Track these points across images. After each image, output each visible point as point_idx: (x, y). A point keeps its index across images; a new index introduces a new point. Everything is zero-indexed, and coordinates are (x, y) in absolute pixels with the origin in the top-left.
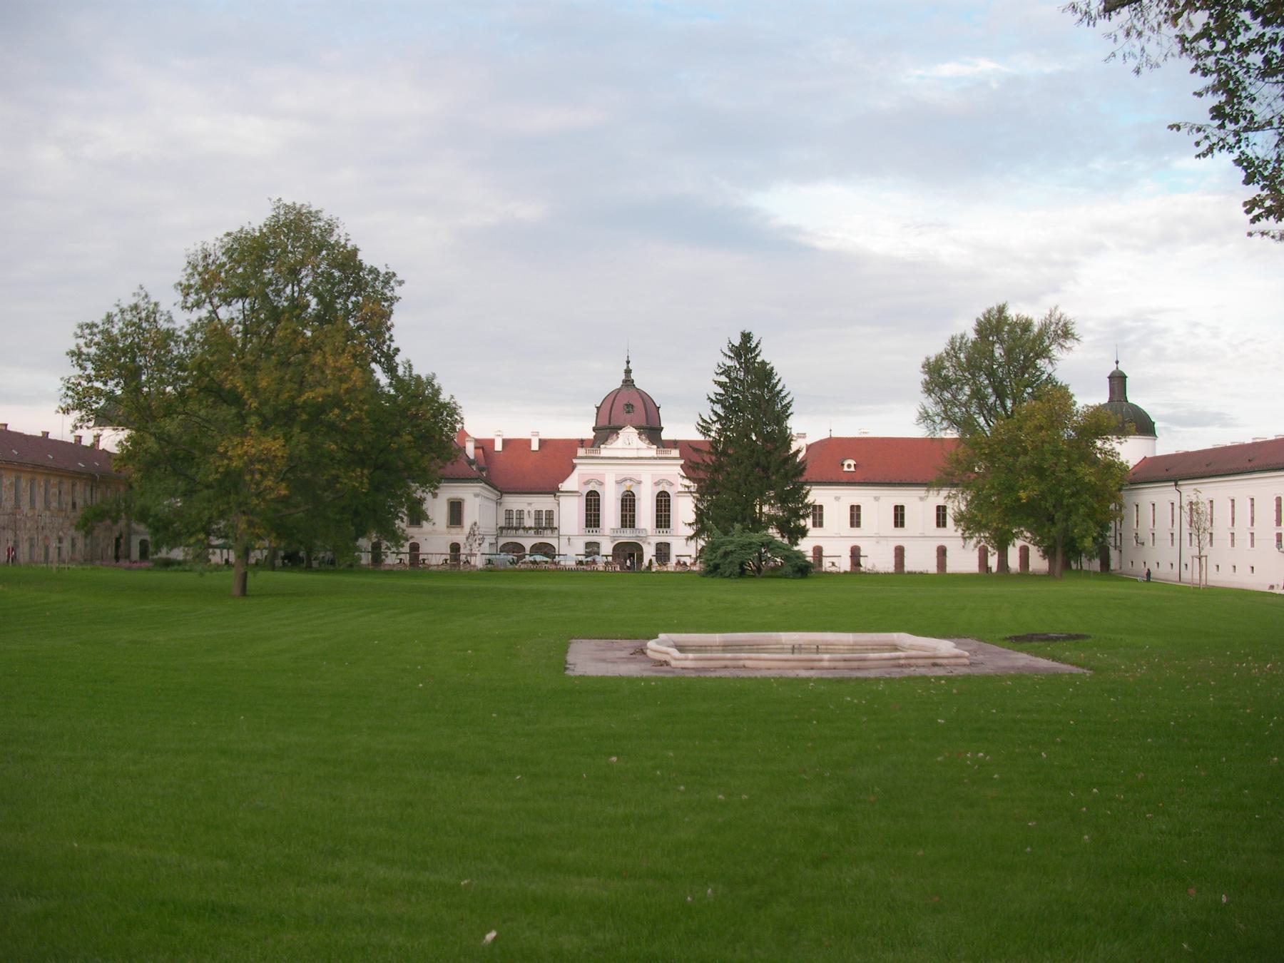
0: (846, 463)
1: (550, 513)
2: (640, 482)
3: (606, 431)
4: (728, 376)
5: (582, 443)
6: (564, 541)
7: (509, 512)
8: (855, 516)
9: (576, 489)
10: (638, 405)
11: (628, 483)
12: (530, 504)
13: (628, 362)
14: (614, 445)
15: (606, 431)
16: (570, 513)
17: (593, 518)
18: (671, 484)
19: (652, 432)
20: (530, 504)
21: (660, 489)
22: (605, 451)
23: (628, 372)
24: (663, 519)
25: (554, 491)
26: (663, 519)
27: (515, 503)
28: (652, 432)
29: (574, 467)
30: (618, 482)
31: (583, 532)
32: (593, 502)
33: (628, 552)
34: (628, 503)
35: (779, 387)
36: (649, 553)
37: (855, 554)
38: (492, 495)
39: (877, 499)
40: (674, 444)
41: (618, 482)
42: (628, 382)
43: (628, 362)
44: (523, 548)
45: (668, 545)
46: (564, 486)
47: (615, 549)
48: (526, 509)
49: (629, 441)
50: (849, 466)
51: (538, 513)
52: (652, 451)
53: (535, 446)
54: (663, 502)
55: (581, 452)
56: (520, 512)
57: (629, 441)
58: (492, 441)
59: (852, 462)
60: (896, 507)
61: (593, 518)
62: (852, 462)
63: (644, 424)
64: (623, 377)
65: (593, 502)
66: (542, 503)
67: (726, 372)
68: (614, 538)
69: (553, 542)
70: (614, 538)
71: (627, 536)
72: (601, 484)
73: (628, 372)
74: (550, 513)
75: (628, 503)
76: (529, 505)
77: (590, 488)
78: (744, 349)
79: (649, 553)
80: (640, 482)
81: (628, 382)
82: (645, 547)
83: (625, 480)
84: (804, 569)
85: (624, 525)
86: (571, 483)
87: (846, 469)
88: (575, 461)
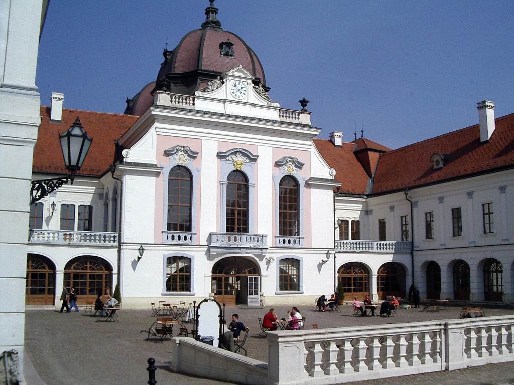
6: (129, 254)
9: (152, 160)
11: (239, 159)
14: (220, 93)
29: (152, 120)
31: (162, 238)
34: (238, 190)
41: (221, 156)
44: (52, 266)
45: (296, 263)
46: (132, 155)
47: (217, 268)
69: (109, 255)
72: (193, 155)
80: (253, 159)
82: (262, 264)
83: (235, 152)
85: (230, 229)
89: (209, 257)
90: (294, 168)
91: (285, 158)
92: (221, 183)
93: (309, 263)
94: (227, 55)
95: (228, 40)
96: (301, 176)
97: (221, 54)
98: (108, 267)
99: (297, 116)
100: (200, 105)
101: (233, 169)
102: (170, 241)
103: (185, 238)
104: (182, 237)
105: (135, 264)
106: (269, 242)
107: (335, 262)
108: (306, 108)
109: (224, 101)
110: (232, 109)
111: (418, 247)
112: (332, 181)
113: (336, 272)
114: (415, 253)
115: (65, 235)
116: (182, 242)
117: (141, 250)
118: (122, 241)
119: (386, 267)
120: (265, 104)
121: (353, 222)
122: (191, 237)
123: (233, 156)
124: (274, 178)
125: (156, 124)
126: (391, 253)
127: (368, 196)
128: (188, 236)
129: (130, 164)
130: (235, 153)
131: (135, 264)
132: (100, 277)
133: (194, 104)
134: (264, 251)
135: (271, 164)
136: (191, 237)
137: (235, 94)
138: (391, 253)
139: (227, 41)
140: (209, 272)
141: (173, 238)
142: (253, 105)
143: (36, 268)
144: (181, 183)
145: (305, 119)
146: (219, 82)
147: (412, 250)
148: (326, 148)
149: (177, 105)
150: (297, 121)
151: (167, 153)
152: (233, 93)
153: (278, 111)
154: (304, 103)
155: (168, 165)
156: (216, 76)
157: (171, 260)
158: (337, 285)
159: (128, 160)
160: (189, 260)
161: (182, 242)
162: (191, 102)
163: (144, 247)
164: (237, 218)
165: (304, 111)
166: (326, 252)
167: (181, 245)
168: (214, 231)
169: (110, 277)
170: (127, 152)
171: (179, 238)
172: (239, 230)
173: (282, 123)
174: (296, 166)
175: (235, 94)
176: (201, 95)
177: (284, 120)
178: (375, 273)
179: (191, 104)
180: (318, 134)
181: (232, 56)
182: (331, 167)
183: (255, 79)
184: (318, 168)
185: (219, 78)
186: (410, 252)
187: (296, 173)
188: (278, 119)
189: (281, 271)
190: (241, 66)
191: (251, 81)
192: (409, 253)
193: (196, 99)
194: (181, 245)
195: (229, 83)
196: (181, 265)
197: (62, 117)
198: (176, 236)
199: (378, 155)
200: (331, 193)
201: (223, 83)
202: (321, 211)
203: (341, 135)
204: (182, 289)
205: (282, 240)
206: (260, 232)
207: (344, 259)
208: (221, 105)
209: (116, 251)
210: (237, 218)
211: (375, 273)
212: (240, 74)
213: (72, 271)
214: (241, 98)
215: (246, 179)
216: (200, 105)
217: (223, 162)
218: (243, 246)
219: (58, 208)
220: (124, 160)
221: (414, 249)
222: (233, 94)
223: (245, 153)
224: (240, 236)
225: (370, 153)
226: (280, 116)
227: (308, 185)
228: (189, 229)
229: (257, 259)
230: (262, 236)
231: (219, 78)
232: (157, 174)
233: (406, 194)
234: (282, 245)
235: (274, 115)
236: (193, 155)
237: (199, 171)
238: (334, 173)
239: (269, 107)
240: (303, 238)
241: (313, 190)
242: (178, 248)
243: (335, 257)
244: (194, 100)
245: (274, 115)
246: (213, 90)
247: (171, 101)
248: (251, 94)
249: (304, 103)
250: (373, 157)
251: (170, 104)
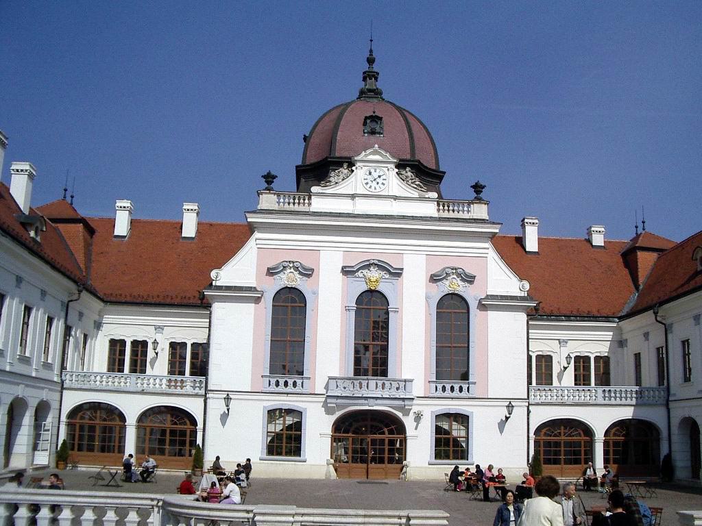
2: (397, 274)
6: (216, 406)
11: (374, 274)
13: (371, 61)
17: (287, 352)
18: (469, 279)
20: (159, 328)
21: (445, 287)
24: (453, 358)
26: (453, 358)
30: (346, 271)
31: (263, 385)
33: (369, 438)
41: (346, 271)
43: (371, 61)
44: (122, 417)
45: (463, 419)
46: (225, 276)
47: (339, 426)
51: (176, 348)
61: (287, 352)
69: (193, 406)
72: (307, 273)
73: (370, 75)
80: (397, 274)
82: (408, 422)
86: (241, 269)
89: (329, 411)
90: (461, 283)
91: (444, 269)
92: (347, 309)
93: (483, 420)
94: (373, 132)
95: (374, 112)
96: (472, 294)
97: (364, 133)
98: (194, 422)
99: (466, 209)
100: (318, 204)
101: (365, 288)
102: (273, 388)
103: (295, 384)
104: (290, 382)
105: (224, 417)
106: (418, 389)
107: (528, 419)
108: (481, 195)
109: (353, 196)
110: (363, 206)
111: (675, 395)
112: (522, 299)
113: (532, 435)
114: (671, 405)
115: (170, 381)
116: (290, 389)
117: (228, 399)
118: (209, 388)
119: (620, 425)
120: (416, 194)
121: (597, 358)
122: (302, 383)
123: (365, 271)
124: (427, 298)
125: (257, 235)
126: (632, 405)
127: (621, 318)
128: (299, 382)
129: (219, 288)
130: (368, 266)
131: (224, 417)
132: (183, 433)
133: (310, 204)
134: (407, 402)
135: (423, 278)
136: (302, 383)
137: (369, 186)
138: (632, 405)
139: (372, 114)
140: (328, 430)
141: (277, 384)
142: (396, 198)
143: (175, 424)
144: (290, 310)
145: (480, 211)
146: (346, 171)
147: (668, 401)
148: (511, 249)
149: (287, 207)
150: (466, 216)
151: (271, 272)
152: (367, 184)
153: (436, 203)
154: (478, 188)
155: (271, 287)
157: (272, 414)
158: (532, 453)
159: (218, 284)
160: (299, 413)
161: (290, 389)
162: (307, 201)
163: (231, 396)
164: (372, 353)
165: (479, 200)
166: (507, 404)
167: (288, 394)
168: (337, 375)
169: (194, 433)
170: (217, 273)
171: (286, 384)
172: (375, 374)
173: (441, 219)
174: (463, 280)
175: (369, 186)
176: (321, 191)
177: (446, 215)
178: (599, 436)
179: (306, 205)
180: (497, 231)
181: (380, 133)
182: (521, 279)
183: (400, 160)
184: (500, 279)
185: (345, 165)
186: (665, 402)
187: (460, 287)
188: (436, 215)
189: (439, 430)
190: (376, 146)
191: (393, 166)
192: (661, 405)
193: (313, 197)
194: (288, 394)
195: (360, 172)
196: (290, 420)
197: (198, 232)
198: (282, 382)
199: (655, 255)
200: (523, 317)
201: (353, 171)
202: (503, 343)
203: (603, 229)
204: (289, 453)
205: (440, 387)
207: (542, 415)
208: (349, 201)
209: (202, 400)
210: (372, 353)
211: (599, 436)
212: (377, 157)
214: (378, 189)
216: (318, 204)
217: (351, 279)
218: (374, 396)
220: (214, 284)
221: (671, 399)
222: (373, 184)
223: (381, 266)
224: (367, 381)
225: (639, 254)
226: (439, 210)
227: (482, 307)
228: (302, 373)
229: (399, 414)
230: (405, 381)
231: (345, 165)
232: (257, 300)
233: (656, 314)
234: (440, 393)
235: (430, 209)
236: (307, 273)
237: (315, 293)
238: (527, 286)
239: (421, 199)
240: (475, 383)
241: (492, 314)
242: (284, 398)
243: (529, 412)
244: (310, 198)
245: (430, 209)
246: (337, 183)
247: (279, 203)
248: (393, 182)
249: (478, 188)
250: (646, 261)
251: (276, 207)
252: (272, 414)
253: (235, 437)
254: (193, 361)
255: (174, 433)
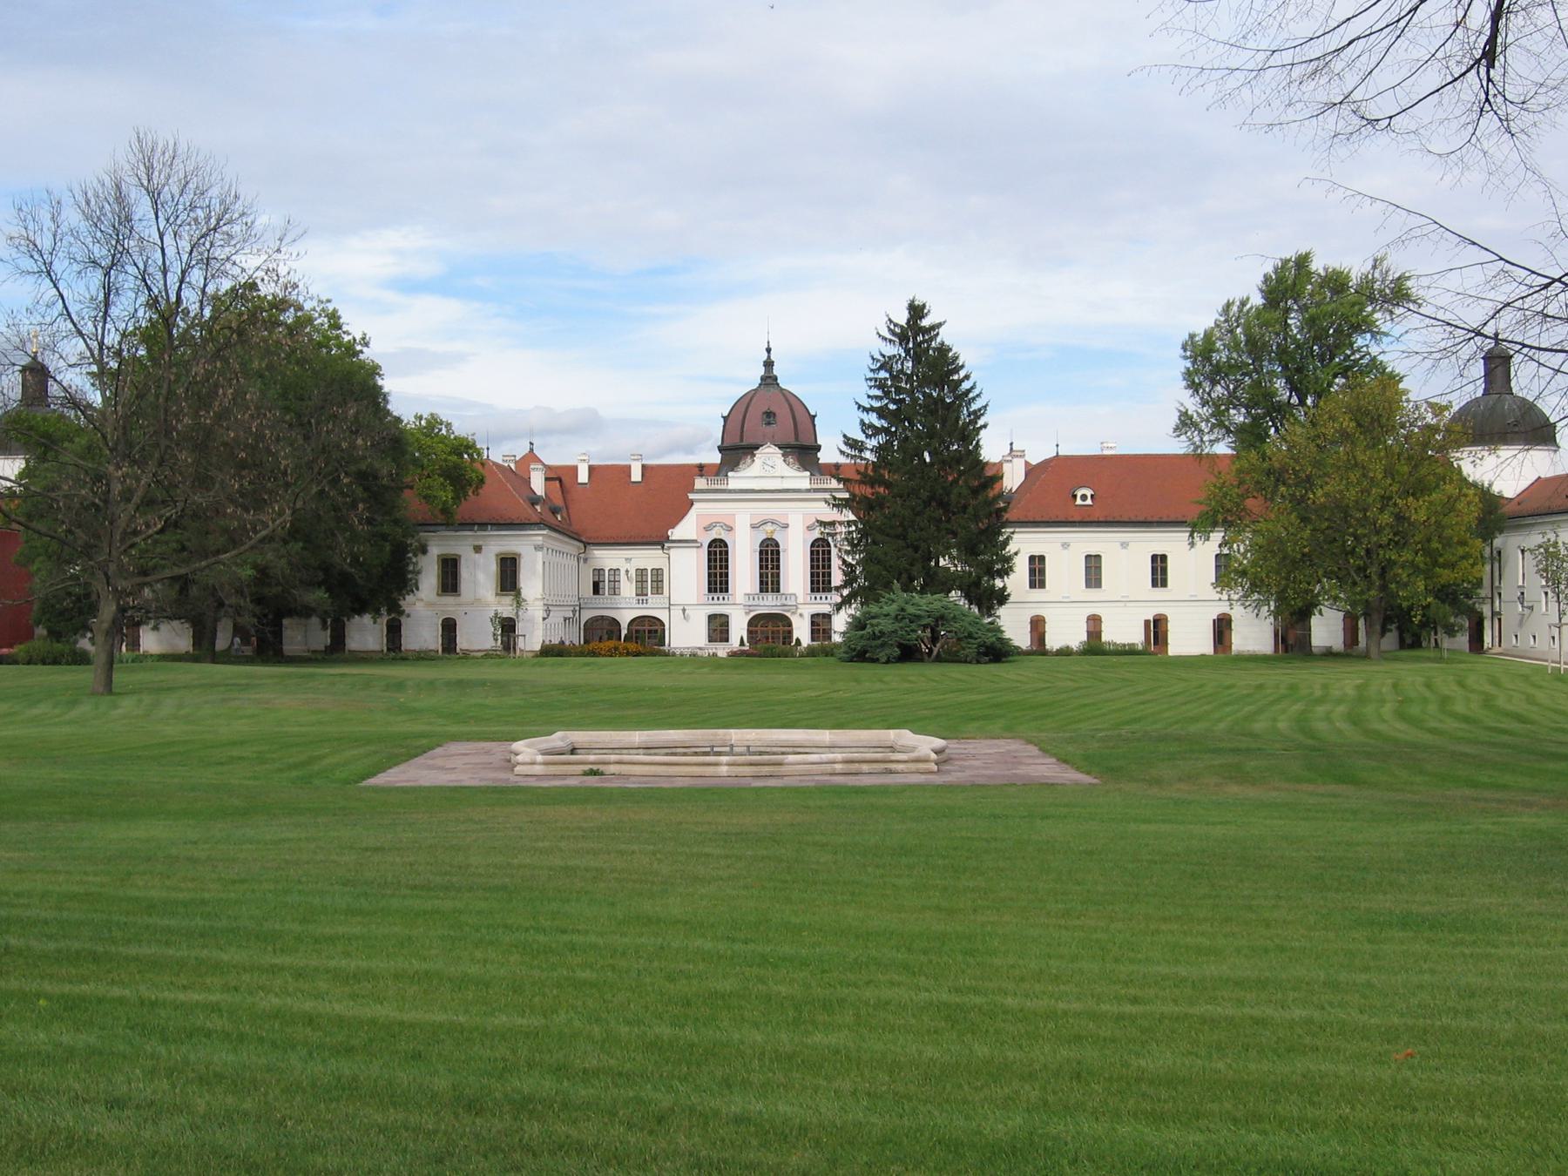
0: (1079, 493)
1: (658, 573)
3: (736, 451)
4: (890, 371)
5: (701, 469)
6: (676, 613)
7: (599, 572)
8: (1093, 567)
10: (783, 413)
11: (769, 527)
12: (628, 560)
13: (769, 350)
15: (736, 451)
16: (685, 570)
17: (718, 581)
19: (803, 451)
22: (736, 480)
23: (769, 364)
25: (660, 541)
26: (820, 582)
27: (608, 558)
28: (803, 451)
29: (691, 503)
30: (753, 527)
32: (718, 555)
34: (770, 556)
35: (966, 386)
36: (802, 632)
37: (1094, 622)
38: (572, 547)
39: (1124, 545)
40: (834, 471)
41: (753, 527)
42: (769, 380)
43: (769, 350)
46: (676, 533)
47: (750, 623)
48: (623, 567)
49: (769, 467)
50: (1084, 497)
51: (641, 573)
52: (802, 480)
53: (636, 476)
54: (819, 554)
55: (700, 483)
56: (616, 571)
57: (769, 467)
58: (574, 469)
59: (1088, 492)
60: (1154, 558)
61: (718, 581)
62: (1088, 492)
63: (793, 442)
64: (761, 371)
65: (718, 555)
66: (647, 558)
67: (886, 364)
68: (749, 608)
69: (662, 615)
70: (749, 608)
71: (769, 604)
72: (730, 529)
73: (769, 364)
74: (658, 573)
75: (770, 556)
76: (619, 560)
77: (714, 535)
78: (914, 331)
79: (802, 632)
80: (786, 526)
81: (769, 380)
82: (794, 620)
84: (997, 651)
85: (764, 587)
86: (685, 529)
87: (1079, 502)
88: (691, 496)
94: (769, 424)
106: (800, 600)
156: (751, 449)
157: (712, 618)
164: (770, 576)
206: (791, 591)
210: (770, 576)
213: (634, 628)
215: (777, 545)
217: (755, 532)
219: (633, 573)
252: (712, 618)
253: (686, 634)
254: (651, 582)
255: (648, 634)
